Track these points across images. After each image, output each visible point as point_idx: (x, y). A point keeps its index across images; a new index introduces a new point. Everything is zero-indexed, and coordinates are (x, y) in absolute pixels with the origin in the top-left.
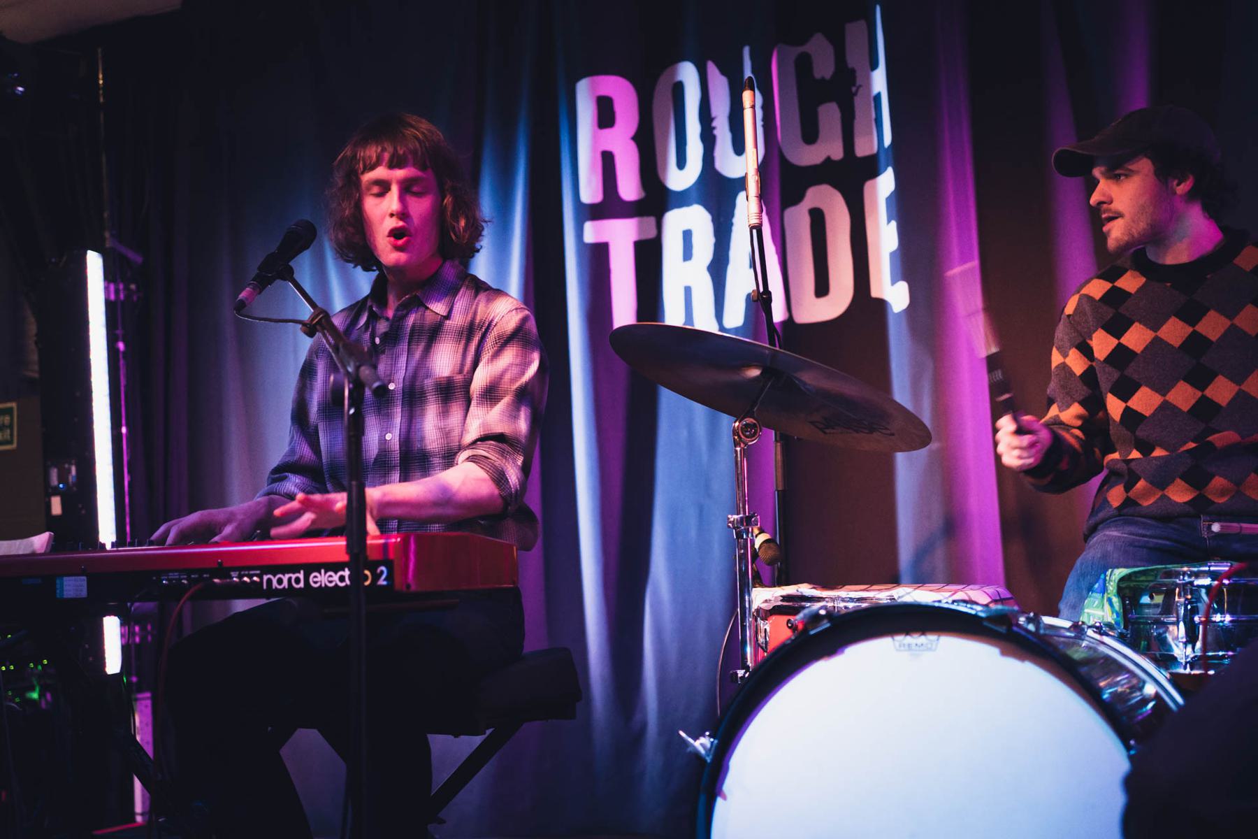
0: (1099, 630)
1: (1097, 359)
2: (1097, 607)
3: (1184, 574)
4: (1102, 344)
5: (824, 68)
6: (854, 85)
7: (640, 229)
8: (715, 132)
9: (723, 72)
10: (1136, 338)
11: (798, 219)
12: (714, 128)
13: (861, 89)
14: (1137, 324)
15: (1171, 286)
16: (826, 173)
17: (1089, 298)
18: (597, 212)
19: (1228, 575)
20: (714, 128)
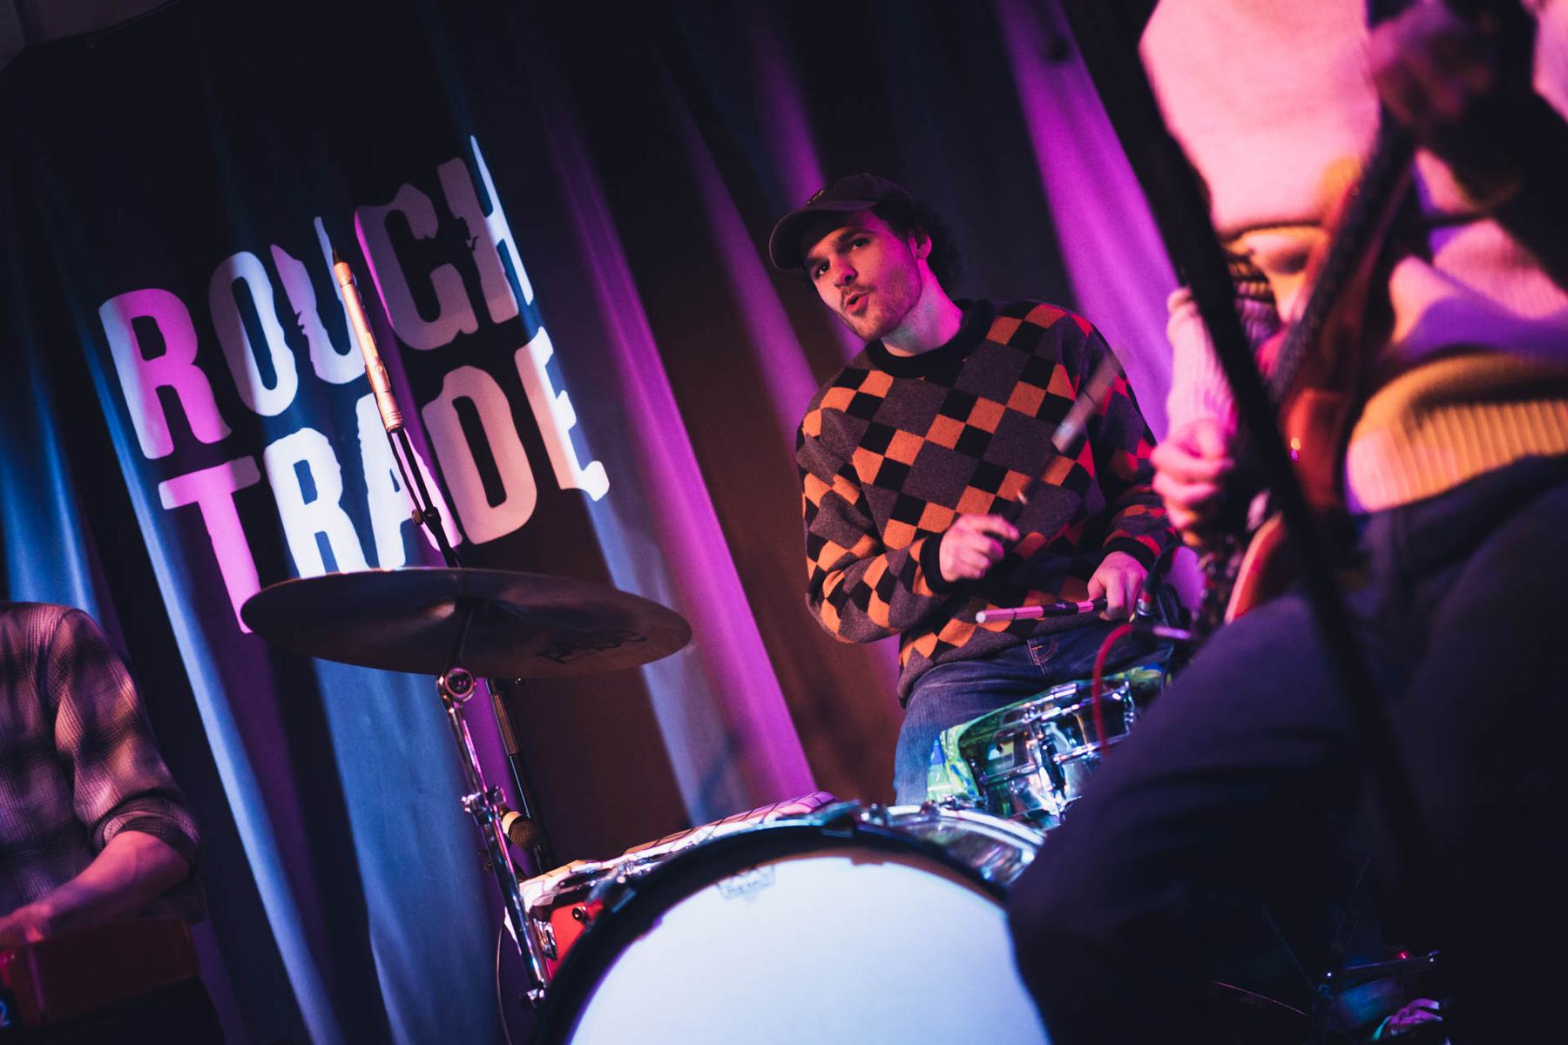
0: (953, 806)
1: (864, 483)
2: (941, 781)
3: (1028, 711)
4: (867, 465)
5: (424, 224)
6: (469, 239)
7: (236, 475)
8: (304, 331)
9: (294, 256)
10: (903, 448)
11: (442, 416)
12: (303, 327)
13: (478, 241)
14: (899, 432)
15: (925, 379)
16: (462, 352)
17: (835, 411)
18: (171, 467)
19: (1074, 699)
20: (303, 327)
